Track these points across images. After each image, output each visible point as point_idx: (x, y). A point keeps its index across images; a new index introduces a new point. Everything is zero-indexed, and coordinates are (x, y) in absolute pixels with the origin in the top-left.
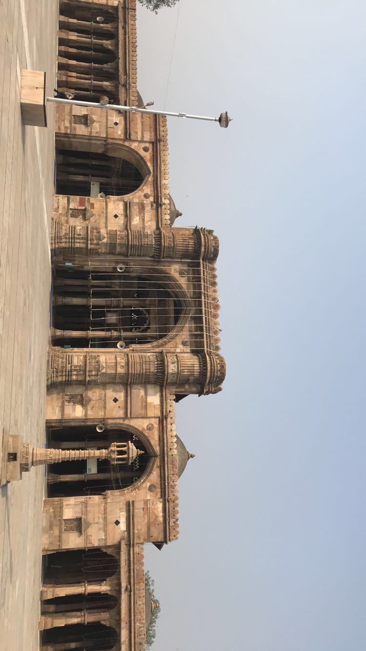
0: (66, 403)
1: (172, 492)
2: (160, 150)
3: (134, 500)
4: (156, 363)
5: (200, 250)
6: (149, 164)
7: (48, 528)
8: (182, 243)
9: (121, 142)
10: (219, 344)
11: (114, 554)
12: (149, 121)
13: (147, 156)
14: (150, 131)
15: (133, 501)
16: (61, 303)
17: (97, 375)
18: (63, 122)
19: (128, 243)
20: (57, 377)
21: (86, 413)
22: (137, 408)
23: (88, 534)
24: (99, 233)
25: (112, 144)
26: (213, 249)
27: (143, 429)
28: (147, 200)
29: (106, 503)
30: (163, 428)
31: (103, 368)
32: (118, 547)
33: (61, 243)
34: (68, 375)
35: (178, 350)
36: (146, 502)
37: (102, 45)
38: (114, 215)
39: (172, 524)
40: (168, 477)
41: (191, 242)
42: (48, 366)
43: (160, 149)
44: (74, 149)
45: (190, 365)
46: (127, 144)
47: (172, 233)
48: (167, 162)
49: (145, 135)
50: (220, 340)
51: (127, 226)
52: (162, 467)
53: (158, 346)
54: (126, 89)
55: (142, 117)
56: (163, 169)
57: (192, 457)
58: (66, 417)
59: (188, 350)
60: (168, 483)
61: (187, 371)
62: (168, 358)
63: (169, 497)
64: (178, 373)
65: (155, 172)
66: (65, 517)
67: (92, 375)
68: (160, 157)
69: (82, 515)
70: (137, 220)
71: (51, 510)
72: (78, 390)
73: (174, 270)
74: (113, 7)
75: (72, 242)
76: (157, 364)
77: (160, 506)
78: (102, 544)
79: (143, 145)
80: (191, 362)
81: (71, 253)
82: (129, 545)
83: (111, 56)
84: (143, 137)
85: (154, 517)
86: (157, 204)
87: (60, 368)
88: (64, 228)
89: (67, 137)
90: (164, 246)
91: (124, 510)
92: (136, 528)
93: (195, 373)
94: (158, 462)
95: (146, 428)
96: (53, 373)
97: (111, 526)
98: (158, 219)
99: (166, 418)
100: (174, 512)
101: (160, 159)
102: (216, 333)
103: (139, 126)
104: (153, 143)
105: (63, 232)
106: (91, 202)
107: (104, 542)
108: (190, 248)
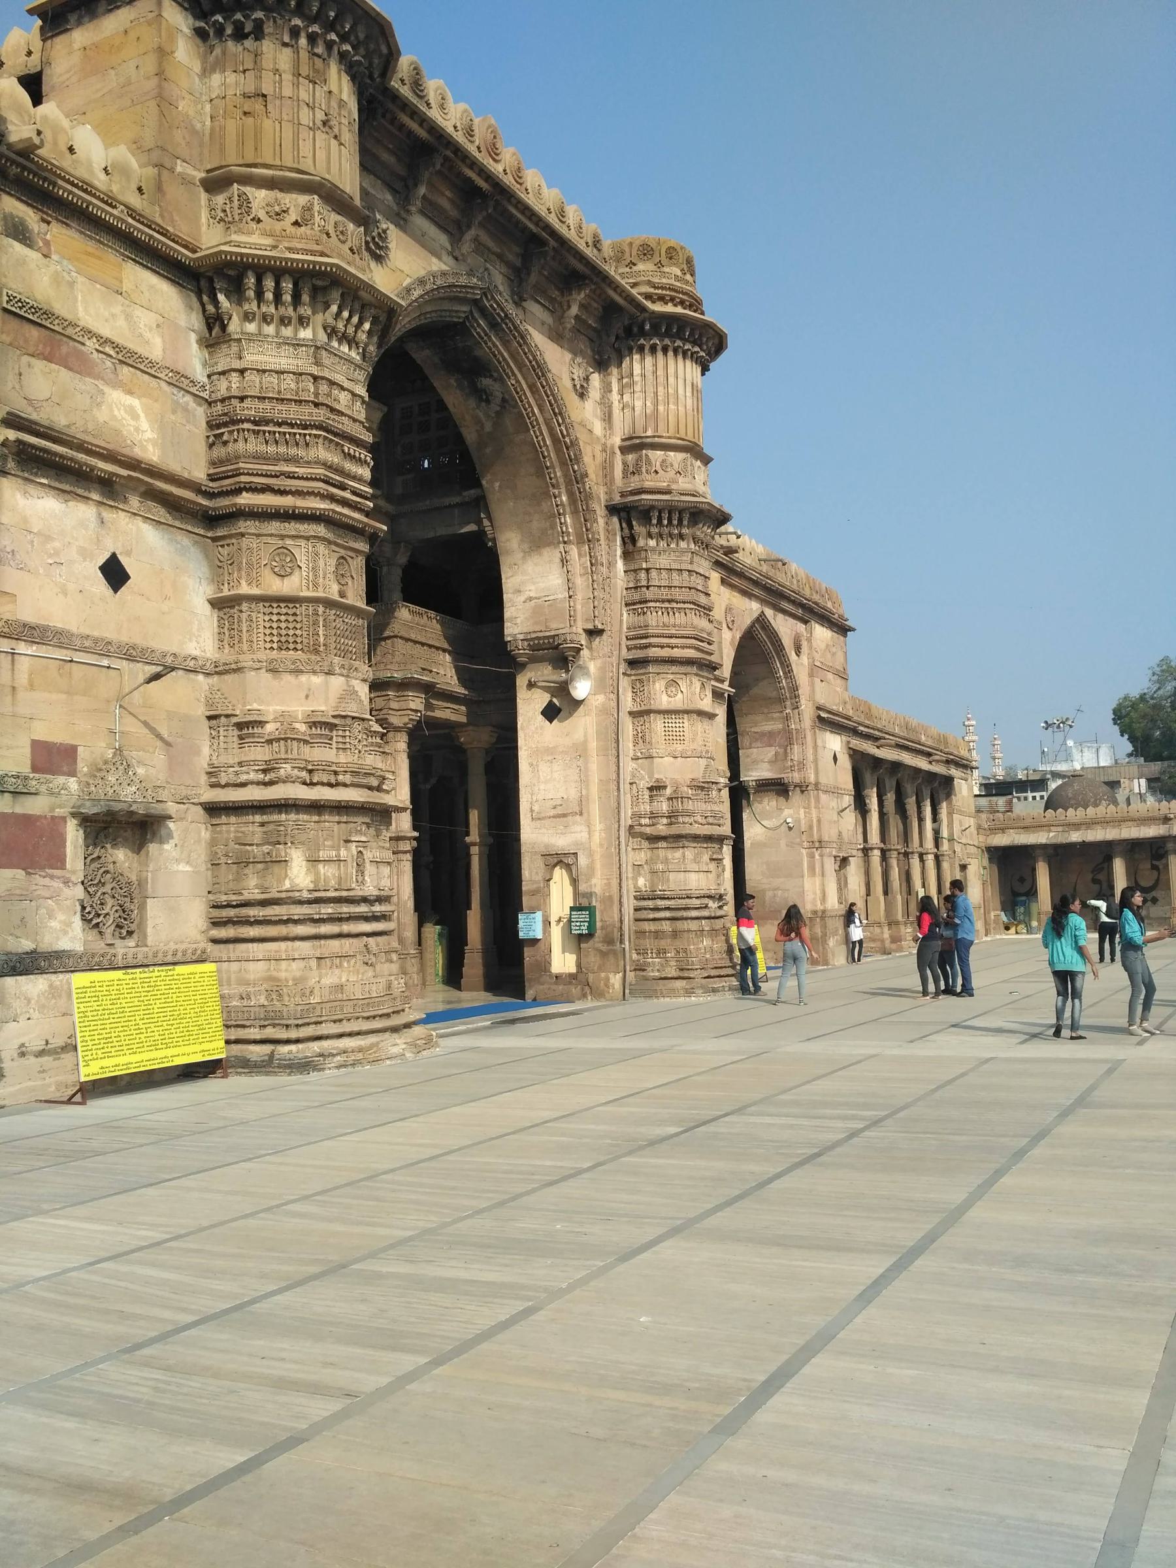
106: (26, 769)
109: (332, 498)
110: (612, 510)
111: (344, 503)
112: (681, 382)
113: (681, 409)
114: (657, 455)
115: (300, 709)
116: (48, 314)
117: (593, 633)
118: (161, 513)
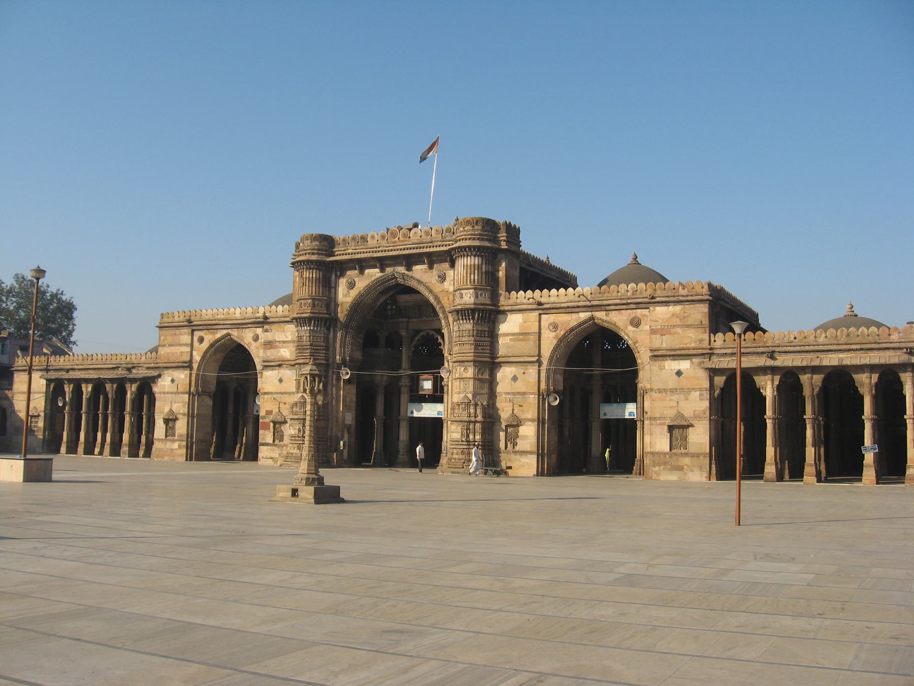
0: (517, 448)
1: (641, 293)
5: (316, 262)
7: (680, 472)
9: (194, 372)
12: (169, 335)
13: (209, 338)
14: (181, 334)
17: (476, 405)
21: (532, 420)
27: (556, 337)
29: (652, 390)
30: (553, 308)
31: (466, 397)
35: (451, 289)
36: (653, 332)
37: (89, 400)
38: (278, 383)
41: (306, 274)
46: (195, 366)
53: (446, 318)
54: (133, 367)
58: (535, 449)
66: (667, 449)
69: (664, 424)
71: (657, 468)
73: (346, 293)
74: (48, 386)
77: (660, 309)
78: (707, 395)
83: (99, 386)
84: (186, 345)
86: (264, 322)
89: (192, 446)
91: (662, 363)
94: (600, 315)
95: (553, 334)
97: (683, 382)
99: (540, 304)
104: (193, 331)
116: (270, 342)
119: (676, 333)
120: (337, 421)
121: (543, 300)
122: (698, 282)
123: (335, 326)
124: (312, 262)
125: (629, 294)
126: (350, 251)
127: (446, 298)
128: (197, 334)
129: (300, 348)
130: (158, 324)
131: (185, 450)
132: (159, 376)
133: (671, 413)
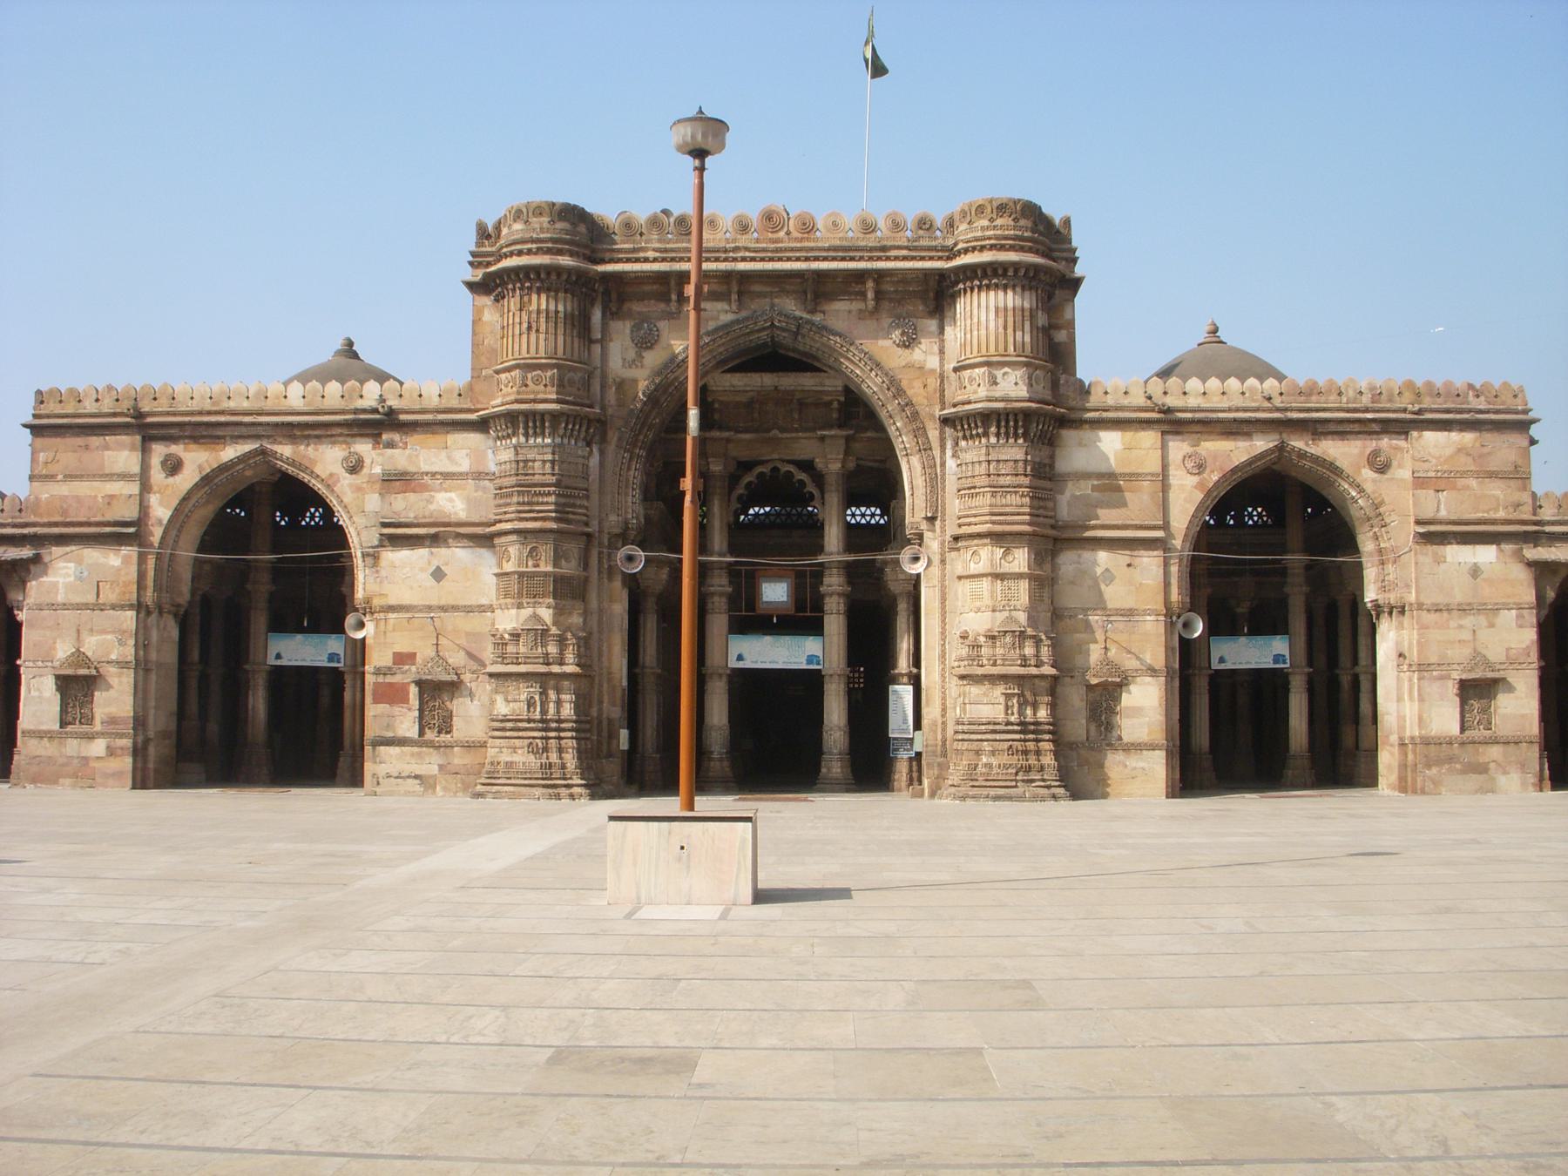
2: (174, 414)
3: (1412, 520)
4: (993, 440)
5: (569, 270)
6: (230, 453)
7: (1482, 777)
8: (542, 336)
10: (910, 217)
11: (1558, 580)
12: (66, 452)
13: (197, 461)
14: (107, 447)
15: (1418, 522)
16: (726, 763)
18: (92, 764)
19: (551, 531)
20: (1042, 769)
21: (1152, 671)
22: (1138, 507)
23: (1504, 659)
24: (518, 635)
25: (158, 587)
26: (559, 225)
27: (1200, 485)
28: (367, 461)
29: (1420, 606)
31: (1011, 619)
32: (1542, 570)
33: (563, 767)
34: (1033, 732)
36: (1419, 482)
39: (1481, 404)
40: (1348, 411)
41: (540, 302)
42: (1010, 798)
43: (168, 414)
44: (173, 726)
45: (1001, 321)
47: (497, 372)
48: (216, 388)
49: (119, 467)
50: (895, 214)
51: (485, 540)
52: (1316, 428)
53: (919, 432)
55: (50, 477)
56: (246, 405)
57: (1215, 331)
58: (1159, 736)
59: (932, 324)
60: (1367, 410)
61: (1019, 334)
62: (973, 398)
63: (1405, 410)
64: (1026, 365)
65: (260, 430)
66: (1455, 729)
67: (1037, 656)
68: (200, 413)
70: (451, 500)
71: (1434, 770)
72: (1076, 699)
75: (559, 730)
76: (998, 435)
77: (1430, 436)
78: (1531, 618)
79: (157, 475)
80: (983, 317)
81: (589, 731)
82: (1534, 538)
84: (124, 477)
85: (1463, 459)
86: (383, 424)
87: (1014, 760)
88: (506, 757)
90: (558, 401)
92: (1492, 515)
93: (1027, 305)
96: (1032, 781)
98: (443, 424)
100: (1448, 394)
101: (209, 413)
102: (868, 227)
103: (83, 488)
104: (148, 440)
105: (523, 758)
106: (390, 664)
107: (1525, 612)
108: (561, 308)
109: (527, 519)
110: (945, 421)
111: (535, 519)
112: (983, 310)
113: (983, 332)
114: (967, 373)
115: (509, 627)
116: (405, 473)
117: (931, 520)
118: (466, 542)
119: (1467, 488)
120: (610, 680)
121: (1171, 401)
122: (1506, 385)
123: (603, 440)
124: (557, 270)
125: (1366, 400)
126: (651, 254)
127: (918, 384)
128: (159, 451)
129: (526, 487)
130: (29, 419)
131: (129, 760)
132: (37, 559)
133: (1460, 654)
